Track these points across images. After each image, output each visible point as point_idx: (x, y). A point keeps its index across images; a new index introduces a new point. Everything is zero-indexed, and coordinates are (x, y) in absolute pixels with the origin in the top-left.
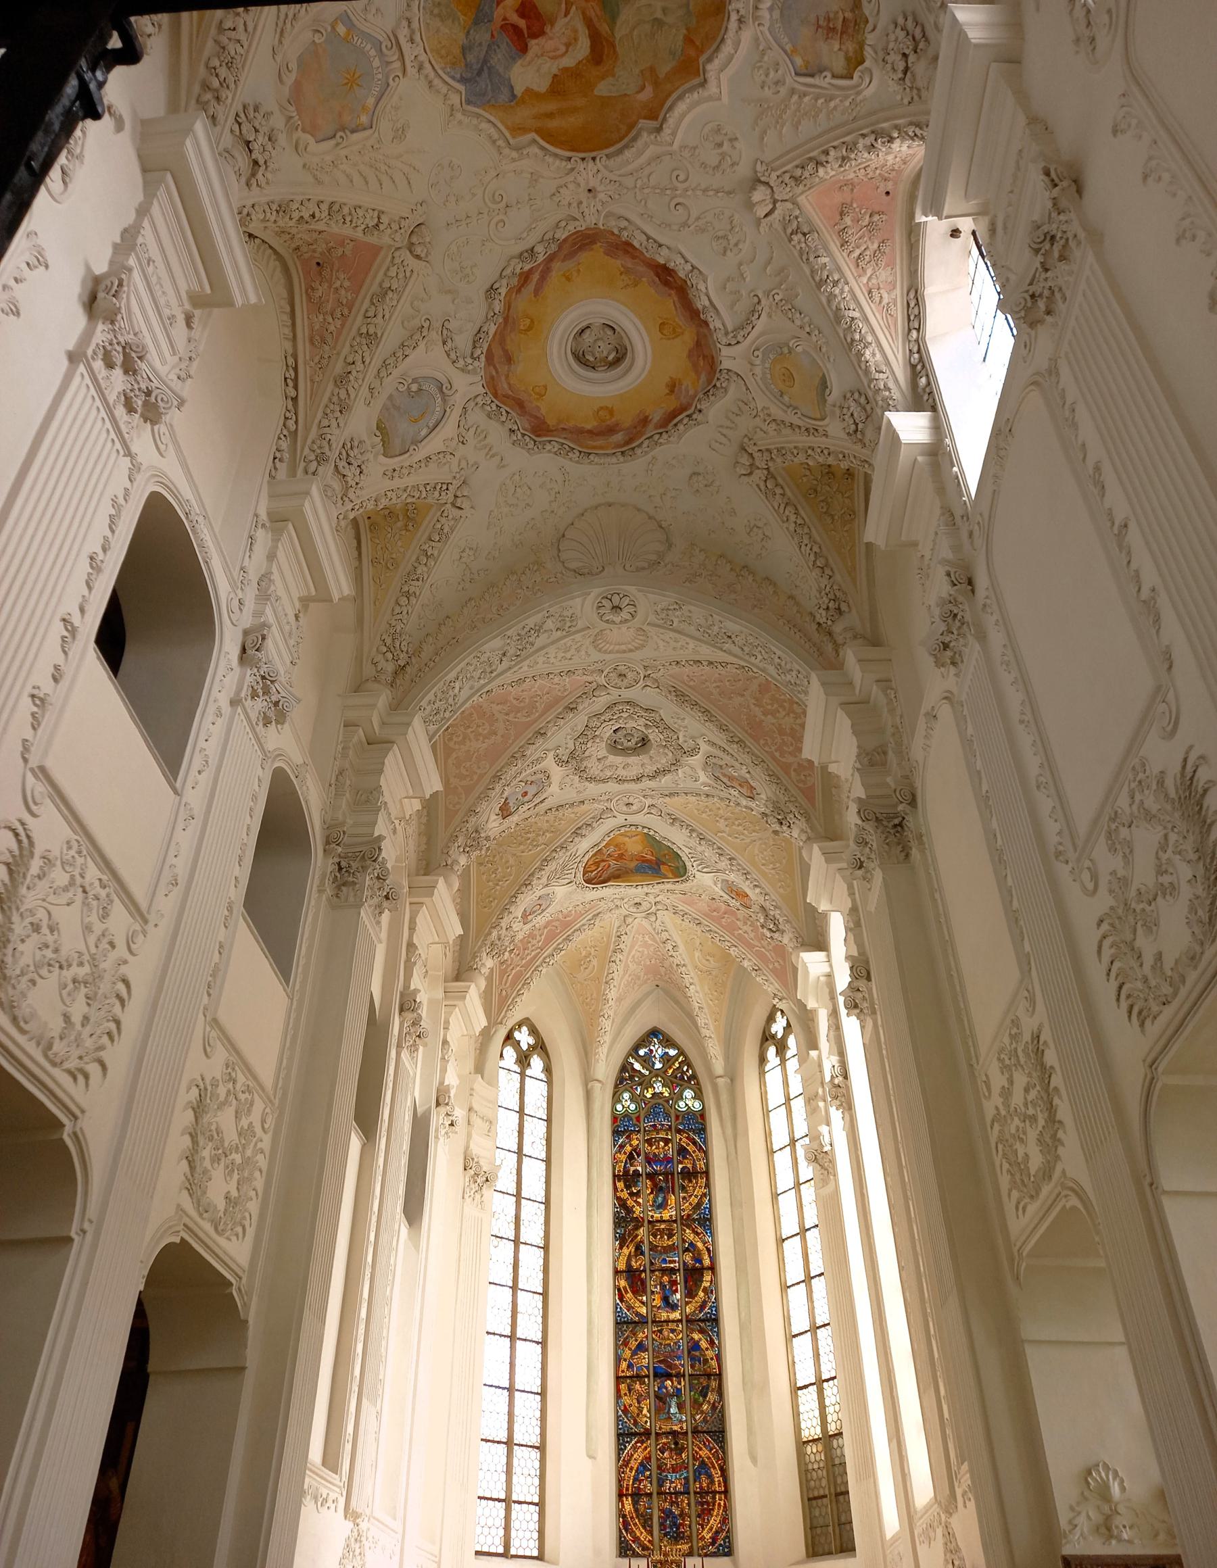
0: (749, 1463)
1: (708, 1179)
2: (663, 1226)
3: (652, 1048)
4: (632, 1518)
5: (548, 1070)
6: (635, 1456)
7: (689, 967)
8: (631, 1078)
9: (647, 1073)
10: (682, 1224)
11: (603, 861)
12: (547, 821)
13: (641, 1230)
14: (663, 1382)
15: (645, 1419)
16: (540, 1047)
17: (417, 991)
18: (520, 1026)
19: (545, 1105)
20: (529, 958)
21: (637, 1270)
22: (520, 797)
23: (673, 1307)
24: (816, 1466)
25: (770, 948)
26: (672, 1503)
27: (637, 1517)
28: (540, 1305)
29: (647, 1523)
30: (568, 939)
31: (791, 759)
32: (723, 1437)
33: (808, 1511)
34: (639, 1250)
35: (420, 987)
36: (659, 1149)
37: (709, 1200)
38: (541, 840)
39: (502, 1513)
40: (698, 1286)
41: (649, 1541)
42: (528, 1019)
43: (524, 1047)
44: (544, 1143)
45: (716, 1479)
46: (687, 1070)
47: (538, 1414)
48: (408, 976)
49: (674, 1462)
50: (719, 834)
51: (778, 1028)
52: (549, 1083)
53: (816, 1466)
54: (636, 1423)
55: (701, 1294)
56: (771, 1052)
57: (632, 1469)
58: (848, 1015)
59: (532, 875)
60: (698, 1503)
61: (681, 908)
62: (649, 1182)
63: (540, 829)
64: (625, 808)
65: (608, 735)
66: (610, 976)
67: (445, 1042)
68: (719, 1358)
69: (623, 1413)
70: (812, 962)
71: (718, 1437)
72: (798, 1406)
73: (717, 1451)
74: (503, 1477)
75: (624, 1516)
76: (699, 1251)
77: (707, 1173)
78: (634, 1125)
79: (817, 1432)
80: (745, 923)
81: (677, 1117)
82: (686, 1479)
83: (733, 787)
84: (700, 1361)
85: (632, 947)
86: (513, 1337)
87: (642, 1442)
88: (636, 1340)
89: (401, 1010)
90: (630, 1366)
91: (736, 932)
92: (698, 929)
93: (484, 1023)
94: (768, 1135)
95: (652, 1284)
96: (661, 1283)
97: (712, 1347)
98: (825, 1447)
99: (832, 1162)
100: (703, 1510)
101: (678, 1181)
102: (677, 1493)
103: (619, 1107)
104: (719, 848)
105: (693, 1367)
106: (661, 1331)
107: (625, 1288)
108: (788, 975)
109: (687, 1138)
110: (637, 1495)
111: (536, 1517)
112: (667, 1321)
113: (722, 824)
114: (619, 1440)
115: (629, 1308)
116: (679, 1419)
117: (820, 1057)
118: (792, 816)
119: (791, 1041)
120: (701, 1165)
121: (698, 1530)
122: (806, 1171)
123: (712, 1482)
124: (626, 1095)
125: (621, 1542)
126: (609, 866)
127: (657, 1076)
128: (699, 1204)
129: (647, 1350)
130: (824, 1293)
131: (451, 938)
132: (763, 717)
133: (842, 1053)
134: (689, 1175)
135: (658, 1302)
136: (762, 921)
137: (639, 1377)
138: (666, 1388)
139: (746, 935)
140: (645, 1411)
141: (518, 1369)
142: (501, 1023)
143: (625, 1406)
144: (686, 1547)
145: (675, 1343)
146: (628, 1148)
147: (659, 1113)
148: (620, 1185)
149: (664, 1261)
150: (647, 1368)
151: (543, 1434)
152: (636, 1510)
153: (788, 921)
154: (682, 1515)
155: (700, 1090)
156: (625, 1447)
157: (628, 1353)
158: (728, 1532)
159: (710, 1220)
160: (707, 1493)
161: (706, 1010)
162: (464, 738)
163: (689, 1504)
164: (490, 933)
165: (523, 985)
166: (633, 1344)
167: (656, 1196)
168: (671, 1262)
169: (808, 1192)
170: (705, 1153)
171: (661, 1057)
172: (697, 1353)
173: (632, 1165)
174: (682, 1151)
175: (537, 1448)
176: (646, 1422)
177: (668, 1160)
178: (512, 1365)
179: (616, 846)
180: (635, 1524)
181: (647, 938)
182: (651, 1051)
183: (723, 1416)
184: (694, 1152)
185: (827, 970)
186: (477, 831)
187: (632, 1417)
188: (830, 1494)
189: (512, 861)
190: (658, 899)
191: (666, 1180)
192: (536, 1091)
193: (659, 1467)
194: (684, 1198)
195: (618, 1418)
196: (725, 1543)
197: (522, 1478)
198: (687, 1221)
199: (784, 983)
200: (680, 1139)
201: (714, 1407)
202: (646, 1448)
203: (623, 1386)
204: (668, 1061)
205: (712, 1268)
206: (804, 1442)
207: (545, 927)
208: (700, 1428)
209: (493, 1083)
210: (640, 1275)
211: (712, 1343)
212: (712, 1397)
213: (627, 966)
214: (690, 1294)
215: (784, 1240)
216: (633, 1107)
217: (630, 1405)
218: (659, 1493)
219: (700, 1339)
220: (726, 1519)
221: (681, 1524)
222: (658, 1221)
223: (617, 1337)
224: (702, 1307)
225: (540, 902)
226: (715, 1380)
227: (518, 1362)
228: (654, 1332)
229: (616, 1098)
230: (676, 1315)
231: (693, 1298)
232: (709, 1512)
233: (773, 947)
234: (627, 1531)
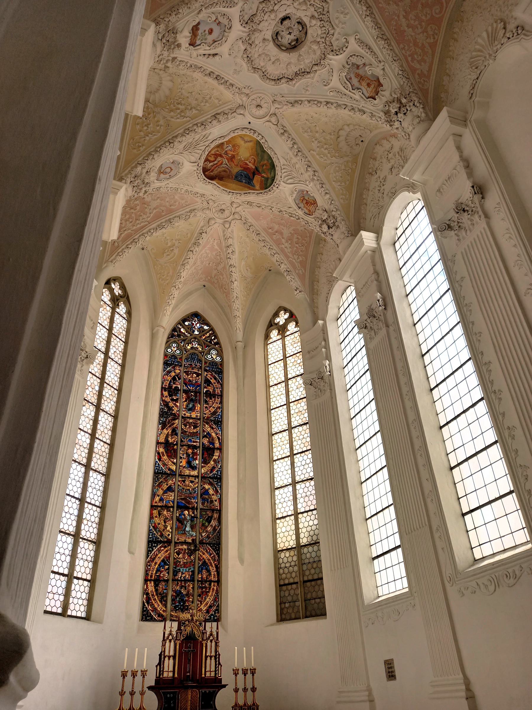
2: (191, 421)
3: (193, 322)
4: (153, 595)
5: (129, 313)
6: (159, 555)
10: (203, 421)
11: (221, 156)
12: (197, 100)
13: (177, 421)
14: (183, 512)
15: (168, 533)
16: (125, 297)
20: (139, 226)
21: (172, 443)
23: (194, 468)
24: (288, 565)
25: (298, 260)
26: (182, 587)
27: (157, 594)
29: (163, 598)
31: (417, 66)
32: (219, 548)
33: (279, 592)
34: (174, 432)
37: (221, 411)
38: (188, 113)
41: (164, 611)
44: (122, 355)
45: (212, 573)
46: (214, 339)
49: (185, 561)
50: (312, 152)
53: (288, 565)
55: (212, 463)
56: (274, 335)
57: (156, 563)
59: (176, 137)
60: (199, 587)
61: (250, 220)
62: (184, 395)
68: (220, 500)
69: (153, 528)
71: (216, 547)
72: (276, 529)
73: (214, 556)
75: (147, 594)
76: (213, 438)
77: (221, 396)
79: (292, 543)
80: (287, 242)
81: (206, 363)
82: (193, 572)
84: (208, 502)
87: (165, 547)
88: (167, 485)
90: (161, 500)
92: (257, 238)
96: (187, 453)
97: (217, 494)
98: (298, 552)
100: (202, 592)
101: (203, 397)
102: (186, 581)
103: (169, 350)
104: (309, 161)
106: (184, 481)
107: (162, 453)
109: (211, 375)
110: (157, 581)
112: (189, 476)
113: (315, 145)
114: (149, 545)
115: (164, 465)
121: (198, 604)
123: (210, 574)
125: (143, 611)
126: (222, 163)
128: (215, 413)
129: (174, 491)
132: (406, 28)
134: (210, 395)
135: (184, 463)
138: (184, 515)
139: (286, 250)
142: (112, 262)
143: (155, 523)
145: (193, 489)
146: (173, 374)
147: (194, 358)
148: (166, 393)
149: (190, 440)
150: (173, 502)
151: (100, 534)
152: (156, 590)
153: (343, 220)
154: (188, 595)
155: (222, 350)
156: (153, 549)
157: (160, 492)
158: (218, 606)
159: (221, 422)
160: (206, 581)
163: (193, 588)
165: (132, 243)
166: (165, 487)
167: (189, 404)
168: (194, 442)
170: (222, 385)
171: (199, 328)
172: (207, 497)
173: (174, 383)
175: (94, 543)
176: (169, 535)
177: (200, 385)
179: (234, 146)
180: (155, 600)
183: (220, 535)
184: (215, 383)
187: (159, 531)
188: (300, 581)
189: (162, 122)
190: (238, 210)
191: (196, 396)
192: (120, 324)
193: (175, 563)
194: (206, 407)
195: (150, 531)
196: (215, 613)
198: (207, 421)
200: (207, 375)
201: (214, 529)
202: (167, 551)
203: (155, 512)
204: (203, 332)
205: (220, 449)
206: (279, 551)
207: (155, 209)
208: (204, 541)
210: (173, 447)
211: (217, 492)
212: (214, 523)
214: (205, 462)
215: (273, 435)
216: (178, 352)
217: (159, 524)
218: (173, 580)
219: (209, 489)
220: (217, 597)
221: (186, 600)
222: (188, 418)
223: (154, 481)
224: (212, 470)
225: (172, 166)
226: (216, 513)
228: (180, 481)
229: (168, 345)
230: (195, 473)
231: (207, 464)
232: (207, 593)
233: (300, 261)
234: (148, 603)
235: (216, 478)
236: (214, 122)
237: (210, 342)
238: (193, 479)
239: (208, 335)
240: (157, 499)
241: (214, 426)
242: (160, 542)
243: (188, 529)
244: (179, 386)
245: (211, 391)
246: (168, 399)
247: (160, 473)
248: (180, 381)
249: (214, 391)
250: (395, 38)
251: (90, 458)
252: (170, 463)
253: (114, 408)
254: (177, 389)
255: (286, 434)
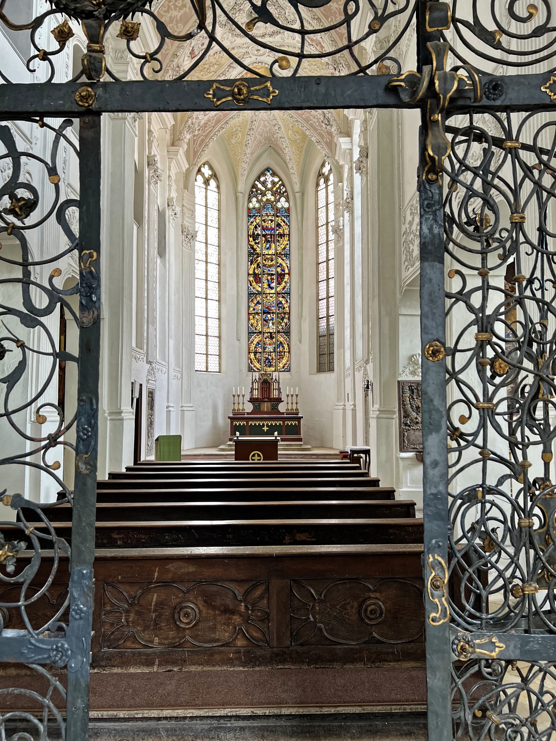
0: (298, 342)
1: (289, 237)
2: (269, 256)
5: (218, 187)
7: (286, 139)
8: (257, 191)
9: (263, 189)
17: (155, 156)
18: (204, 165)
19: (217, 203)
22: (200, 46)
23: (272, 288)
26: (269, 355)
28: (217, 287)
29: (259, 361)
30: (226, 123)
35: (156, 153)
36: (269, 224)
37: (290, 247)
38: (212, 69)
39: (205, 358)
40: (282, 281)
42: (208, 162)
43: (207, 176)
47: (218, 326)
48: (150, 148)
50: (304, 70)
51: (326, 170)
52: (219, 193)
54: (256, 329)
55: (284, 283)
56: (322, 181)
58: (356, 173)
63: (211, 63)
64: (256, 52)
65: (247, 9)
66: (247, 142)
67: (169, 176)
68: (289, 307)
70: (343, 142)
74: (205, 347)
77: (289, 235)
78: (257, 213)
83: (313, 45)
85: (259, 127)
86: (206, 299)
89: (148, 165)
90: (254, 309)
91: (310, 122)
93: (187, 166)
94: (317, 219)
95: (264, 279)
99: (343, 233)
102: (270, 352)
105: (279, 310)
106: (266, 297)
108: (331, 146)
110: (255, 353)
111: (218, 359)
112: (269, 294)
115: (254, 288)
116: (272, 328)
117: (343, 186)
118: (341, 65)
119: (331, 177)
120: (286, 232)
122: (332, 236)
124: (254, 200)
127: (269, 190)
128: (285, 248)
130: (333, 284)
131: (169, 126)
133: (352, 188)
134: (281, 236)
135: (266, 286)
136: (322, 119)
137: (257, 313)
140: (259, 325)
141: (209, 310)
144: (273, 369)
146: (255, 223)
148: (251, 239)
149: (269, 270)
152: (255, 357)
154: (272, 359)
155: (288, 198)
157: (253, 305)
159: (289, 254)
161: (293, 160)
162: (168, 9)
164: (188, 121)
165: (205, 146)
166: (255, 302)
169: (332, 245)
174: (279, 225)
178: (207, 309)
181: (266, 123)
182: (266, 179)
185: (350, 147)
186: (178, 67)
191: (271, 238)
197: (212, 347)
199: (331, 151)
201: (286, 324)
203: (251, 317)
205: (289, 274)
209: (193, 193)
211: (287, 302)
212: (285, 320)
213: (256, 137)
216: (257, 205)
223: (249, 299)
224: (284, 289)
227: (209, 308)
235: (287, 293)
236: (231, 70)
237: (280, 192)
238: (272, 295)
239: (278, 186)
240: (251, 309)
241: (284, 258)
242: (256, 333)
243: (271, 325)
244: (259, 232)
245: (282, 232)
246: (253, 243)
247: (253, 294)
248: (260, 228)
249: (283, 231)
250: (324, 15)
251: (207, 294)
252: (258, 287)
253: (217, 259)
254: (258, 235)
255: (325, 264)
